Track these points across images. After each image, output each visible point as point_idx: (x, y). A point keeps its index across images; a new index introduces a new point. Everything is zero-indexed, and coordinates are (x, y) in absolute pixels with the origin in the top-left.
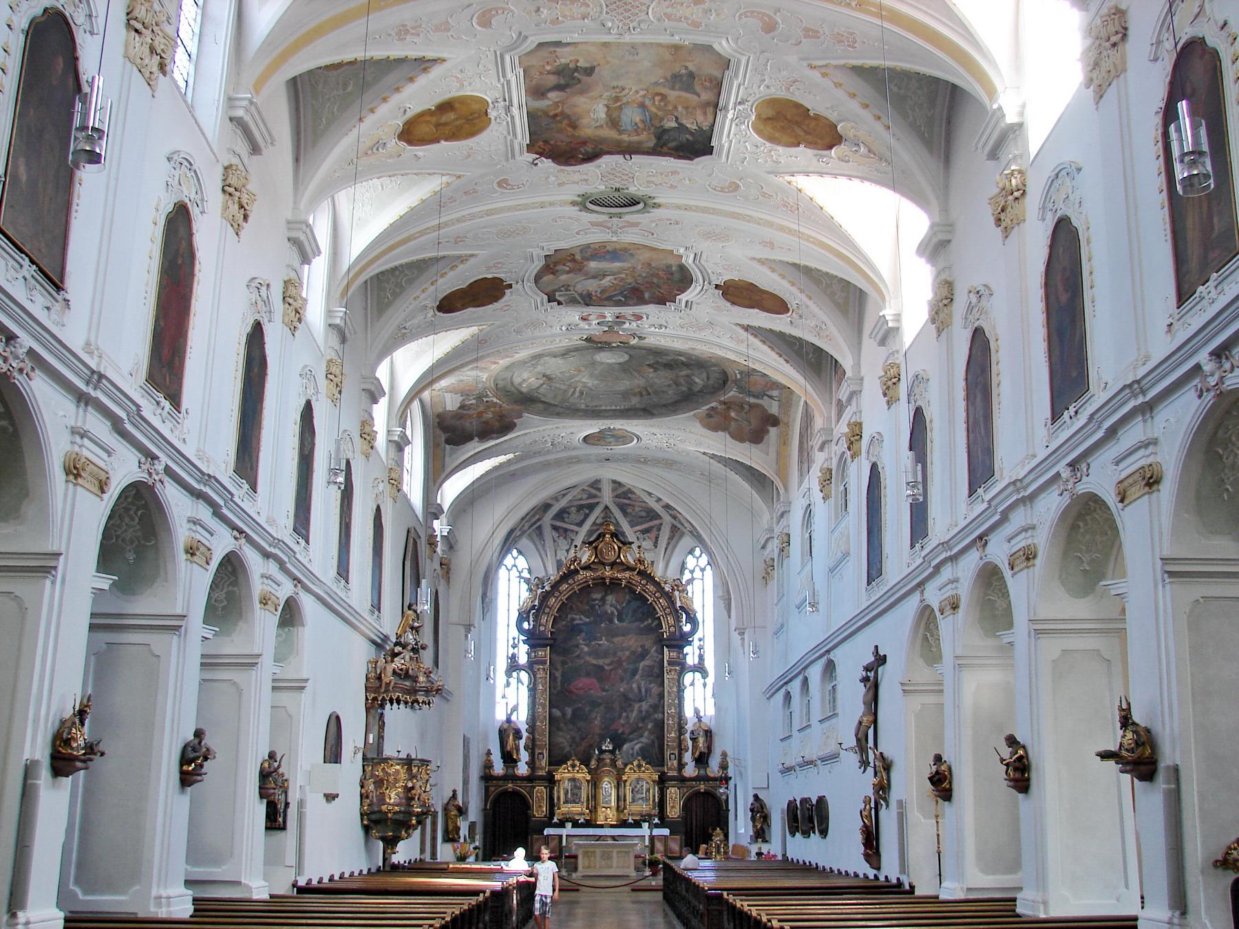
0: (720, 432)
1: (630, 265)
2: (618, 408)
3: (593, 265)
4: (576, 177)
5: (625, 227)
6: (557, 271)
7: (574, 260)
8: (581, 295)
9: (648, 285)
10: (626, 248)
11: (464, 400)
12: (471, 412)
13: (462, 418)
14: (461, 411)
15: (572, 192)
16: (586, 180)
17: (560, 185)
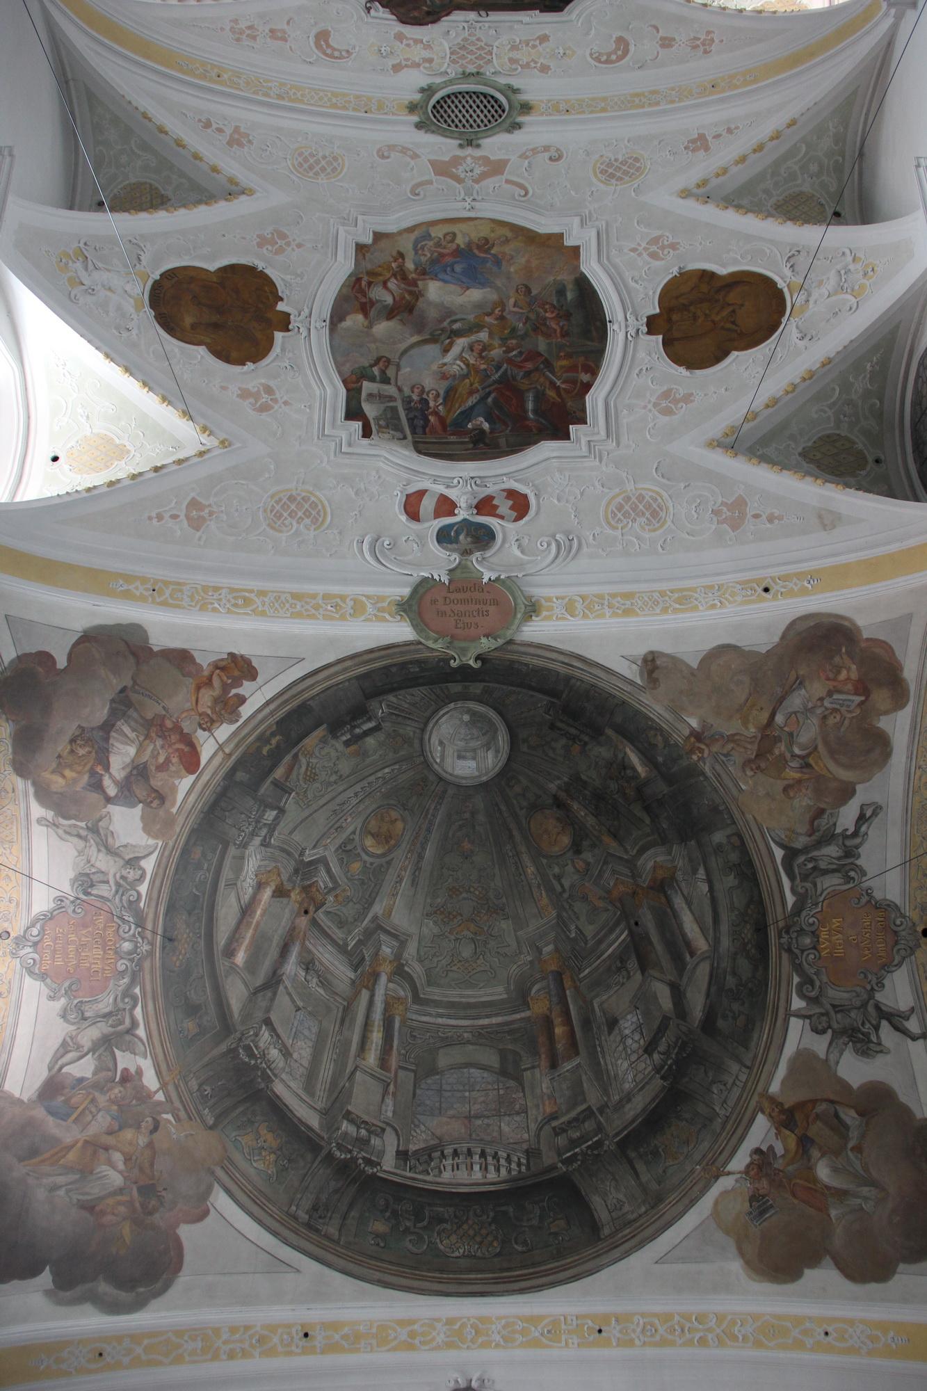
0: (808, 1273)
1: (494, 297)
2: (492, 1176)
3: (434, 291)
4: (418, 53)
5: (484, 176)
6: (372, 303)
7: (402, 274)
8: (407, 401)
9: (529, 365)
10: (487, 240)
11: (64, 1047)
12: (68, 1133)
13: (34, 1152)
14: (40, 1113)
15: (412, 82)
16: (430, 61)
17: (397, 68)
